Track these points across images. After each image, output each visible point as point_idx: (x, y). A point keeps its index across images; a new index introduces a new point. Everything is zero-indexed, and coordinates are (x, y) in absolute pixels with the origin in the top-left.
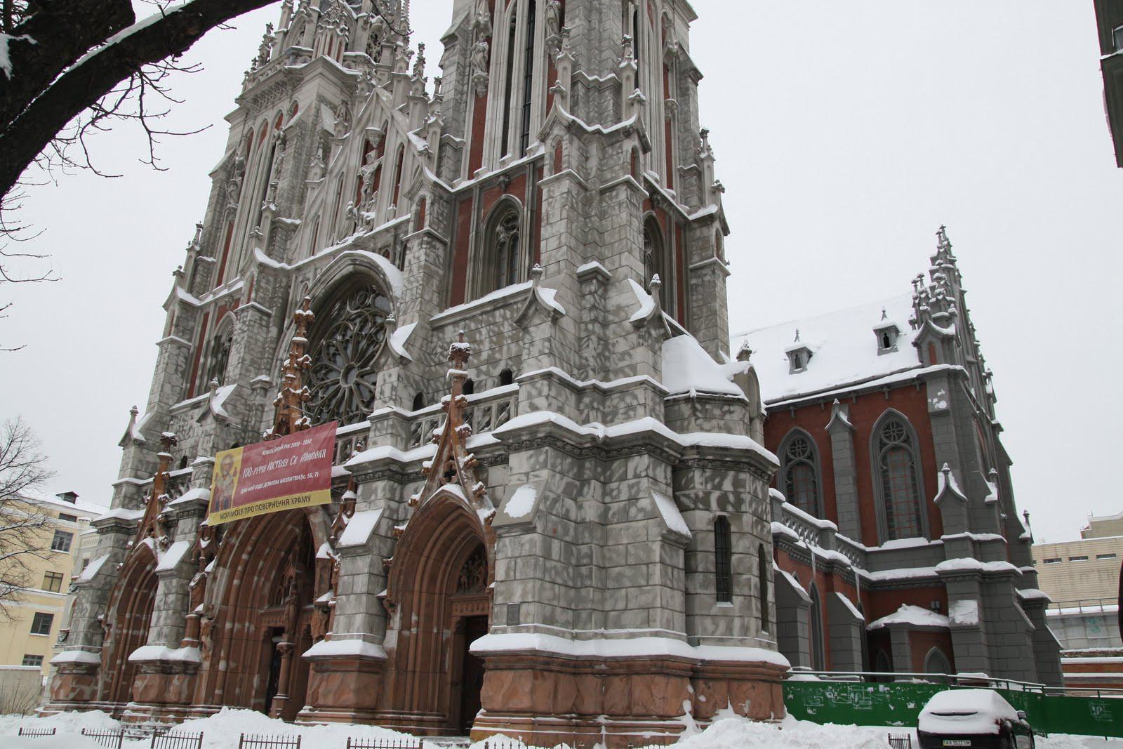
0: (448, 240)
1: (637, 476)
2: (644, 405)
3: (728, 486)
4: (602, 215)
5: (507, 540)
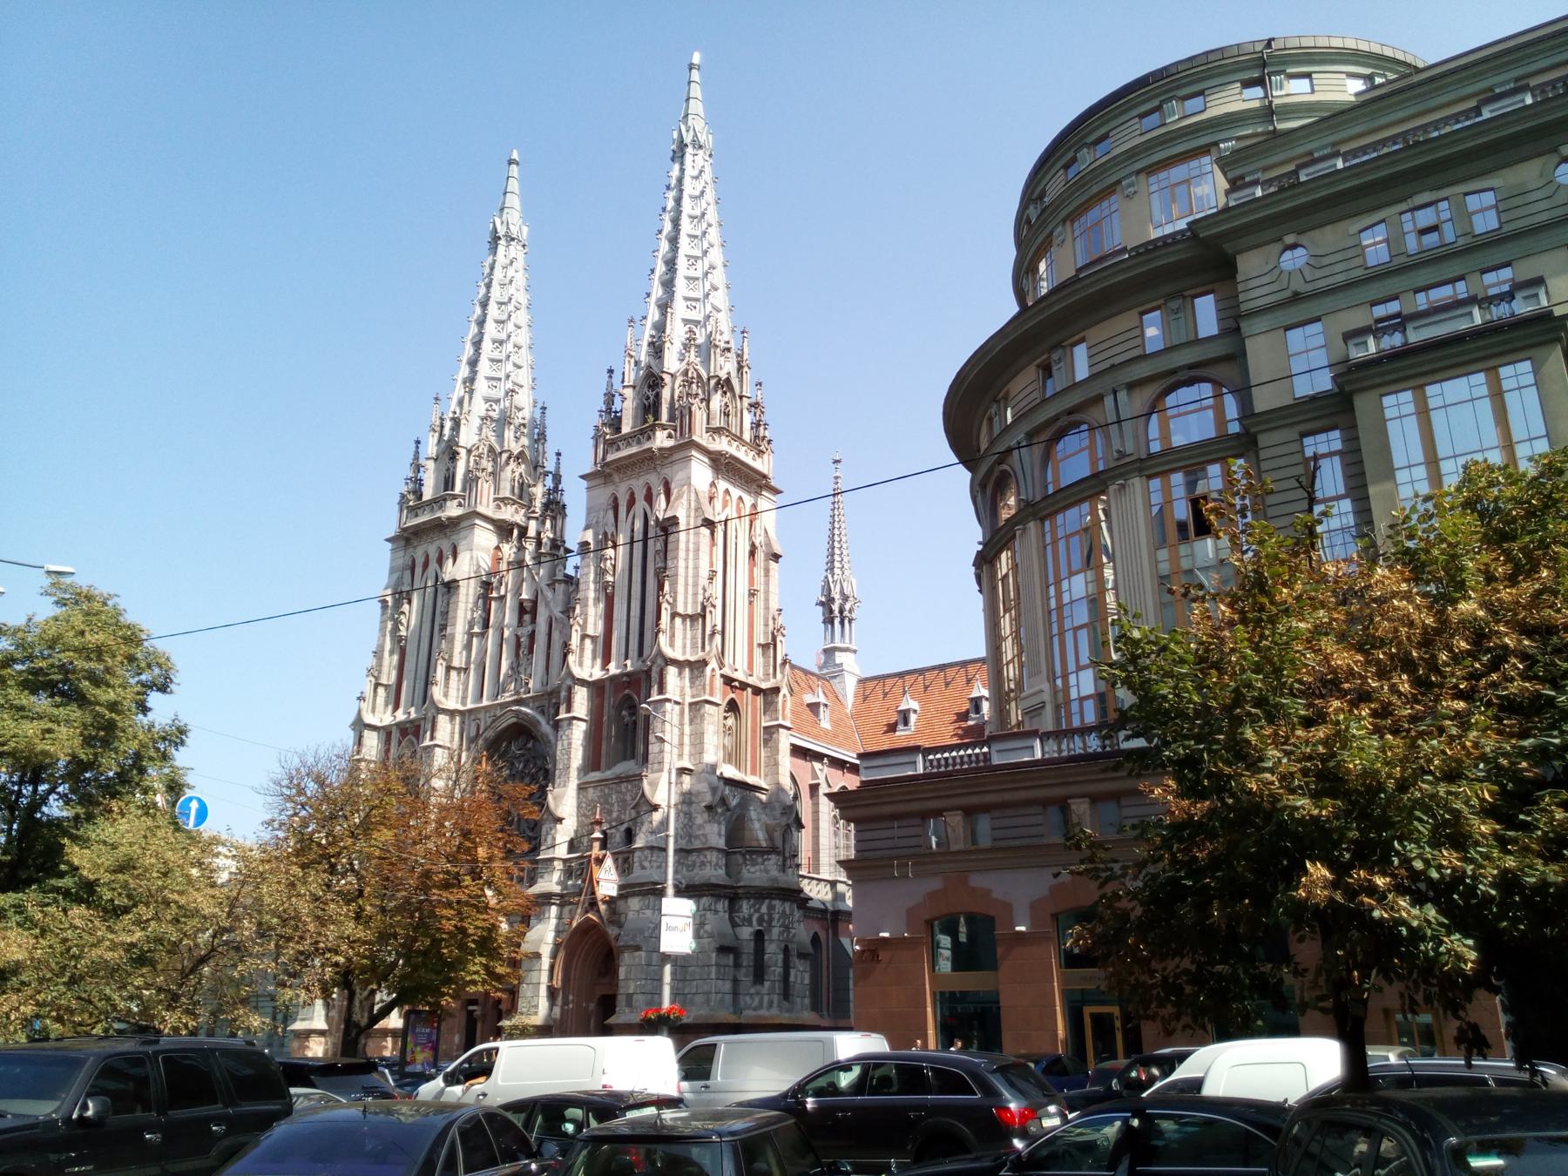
3: (764, 909)
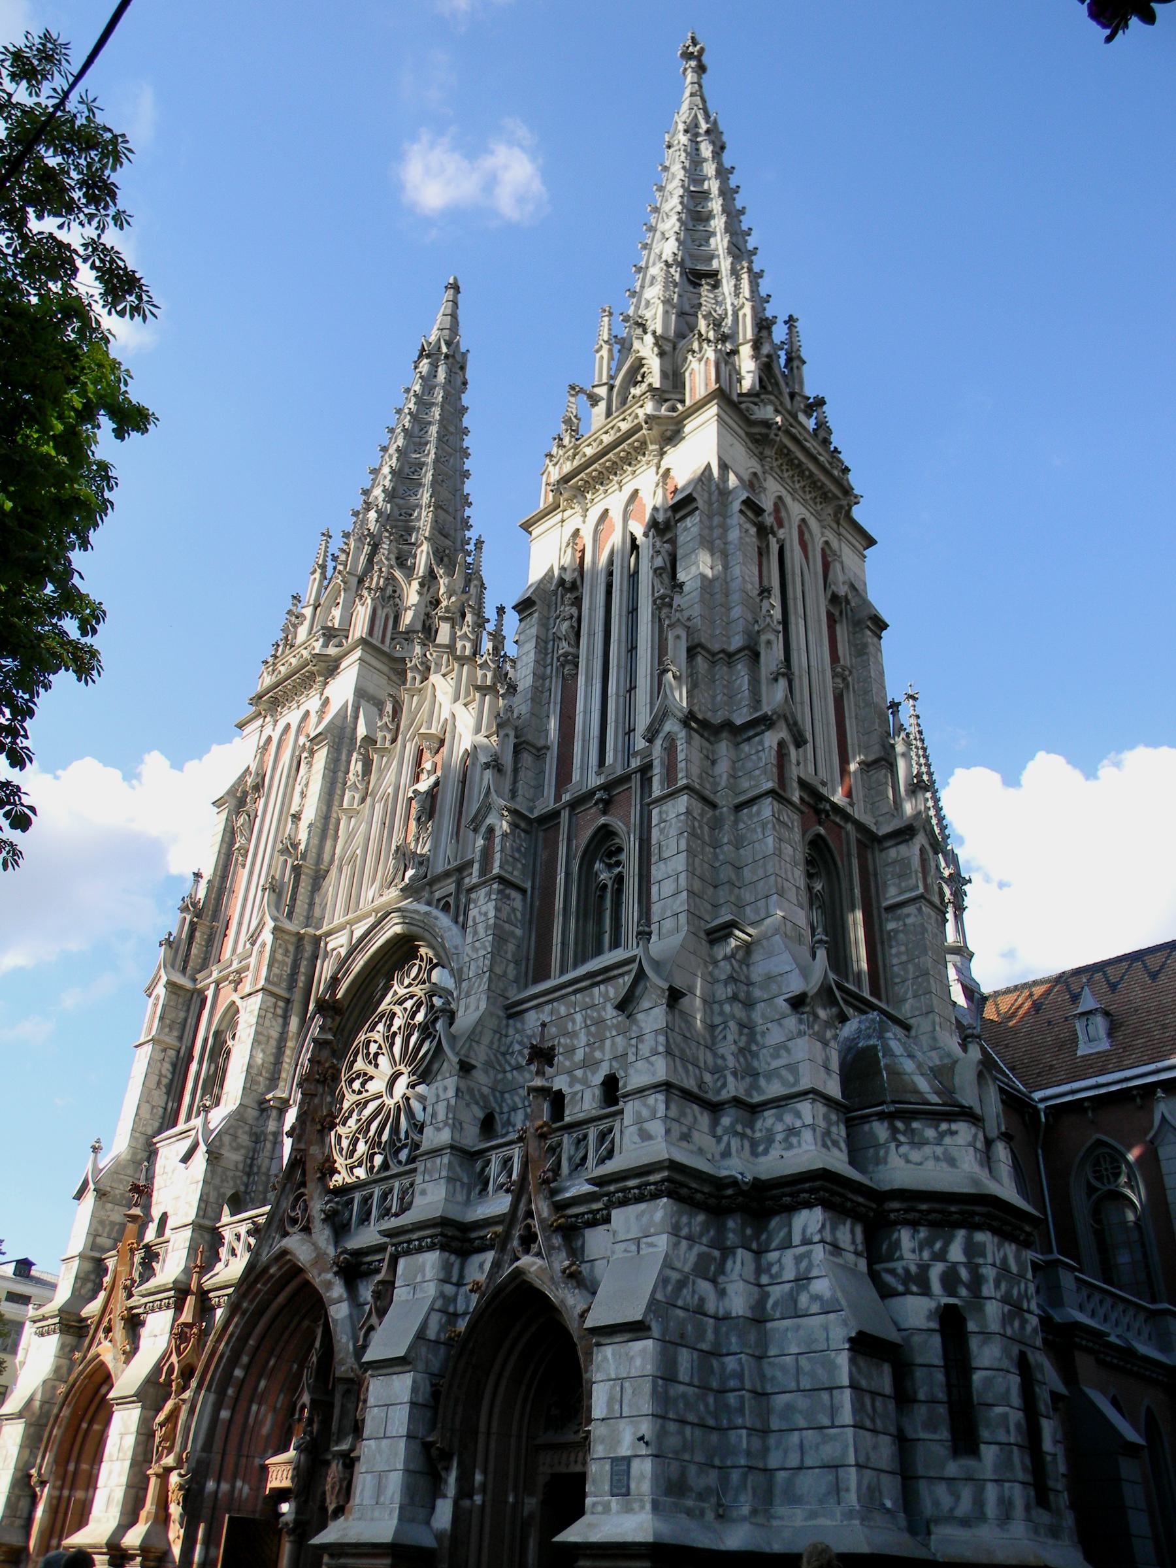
0: (528, 885)
1: (806, 1242)
2: (813, 1127)
3: (956, 1253)
4: (738, 843)
5: (608, 1351)
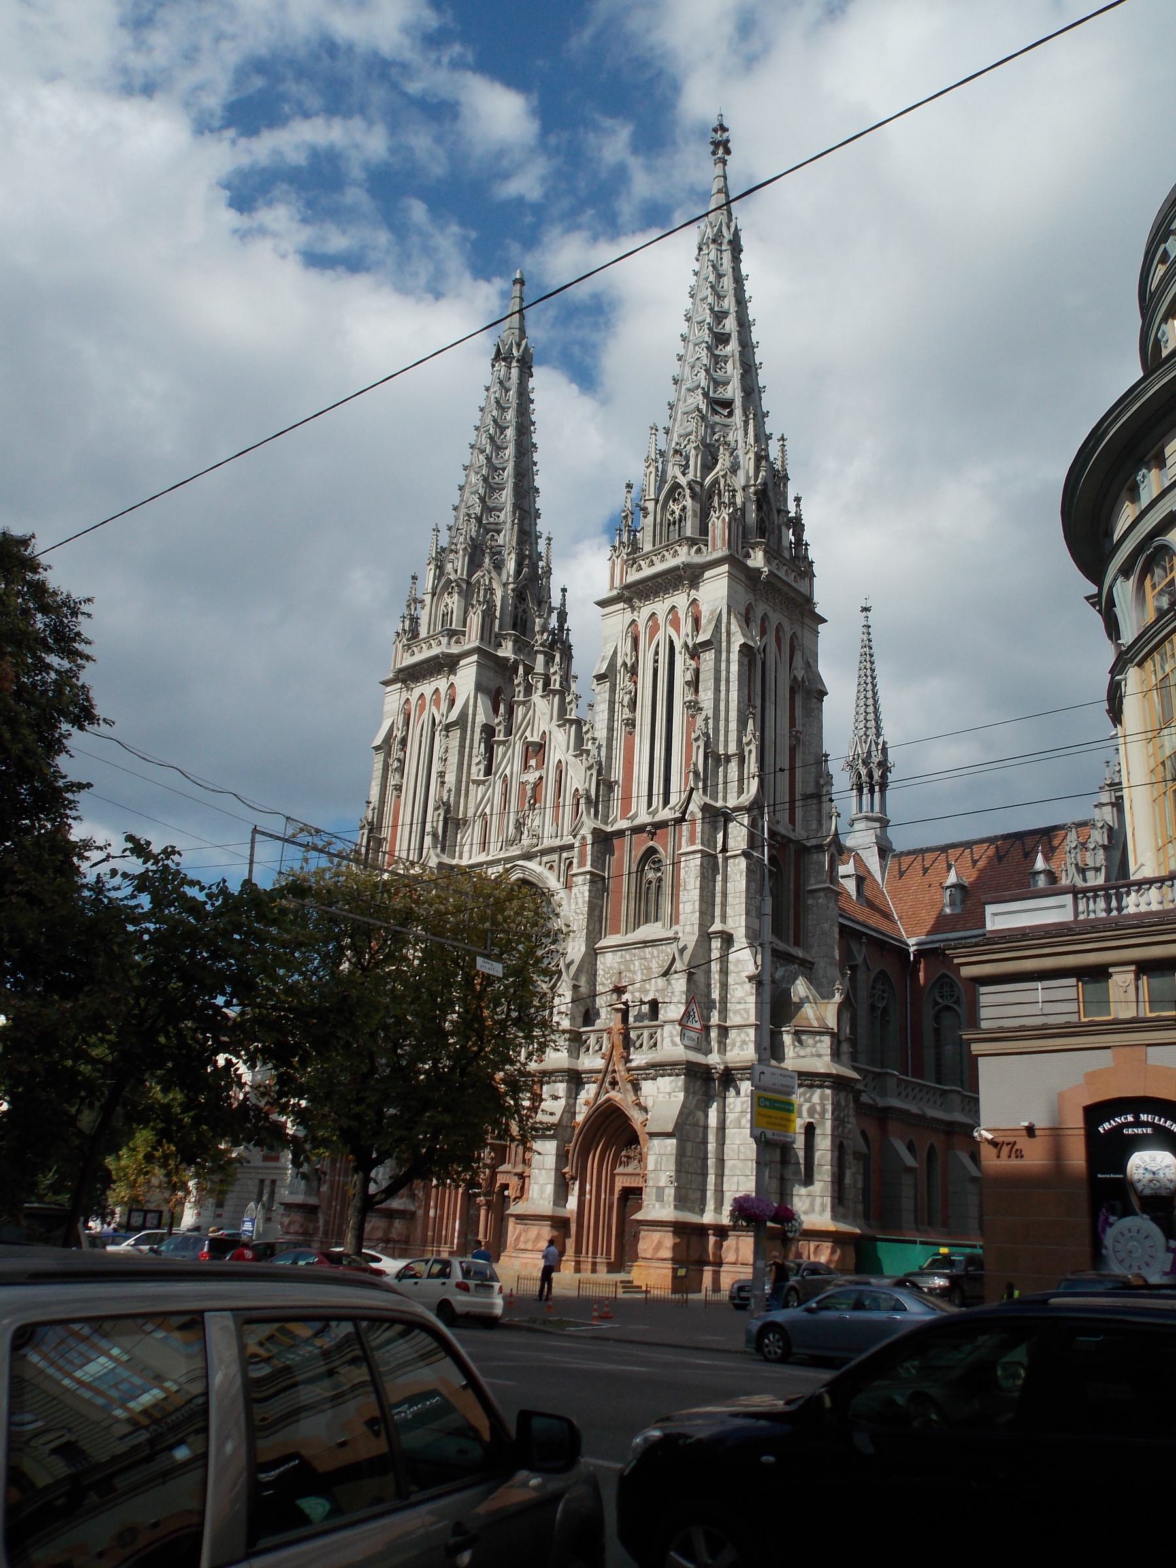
3: (816, 1099)
